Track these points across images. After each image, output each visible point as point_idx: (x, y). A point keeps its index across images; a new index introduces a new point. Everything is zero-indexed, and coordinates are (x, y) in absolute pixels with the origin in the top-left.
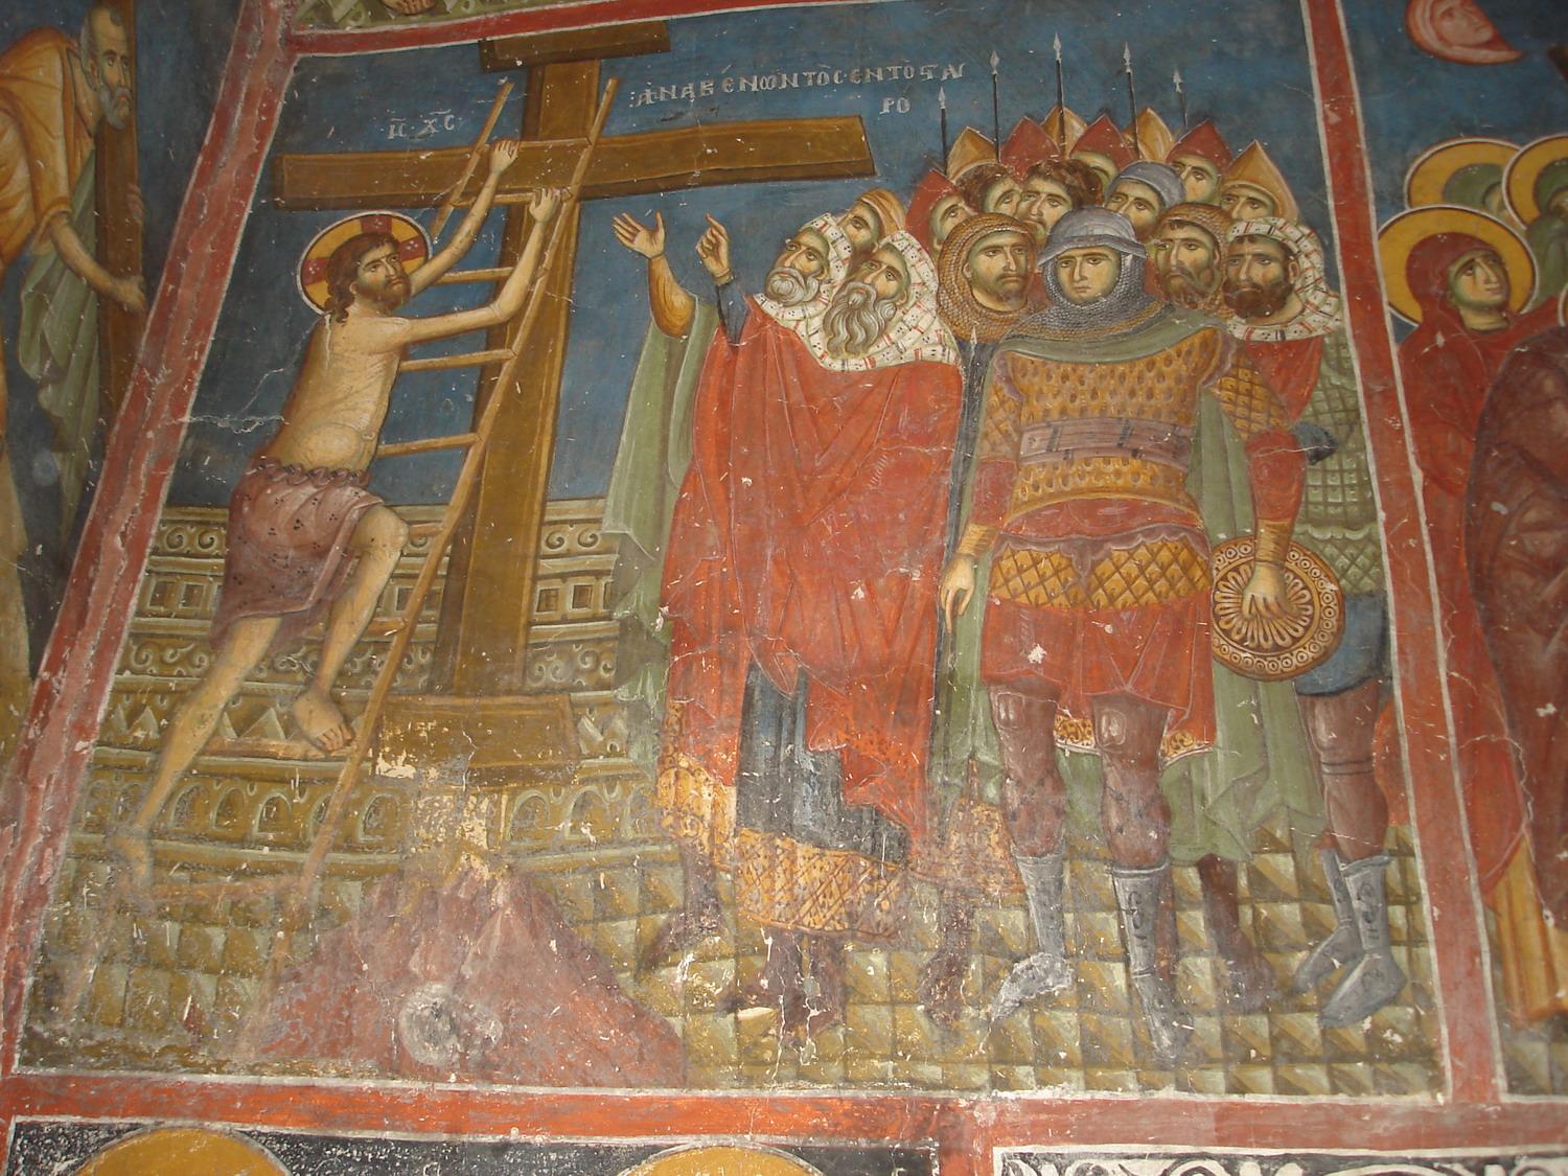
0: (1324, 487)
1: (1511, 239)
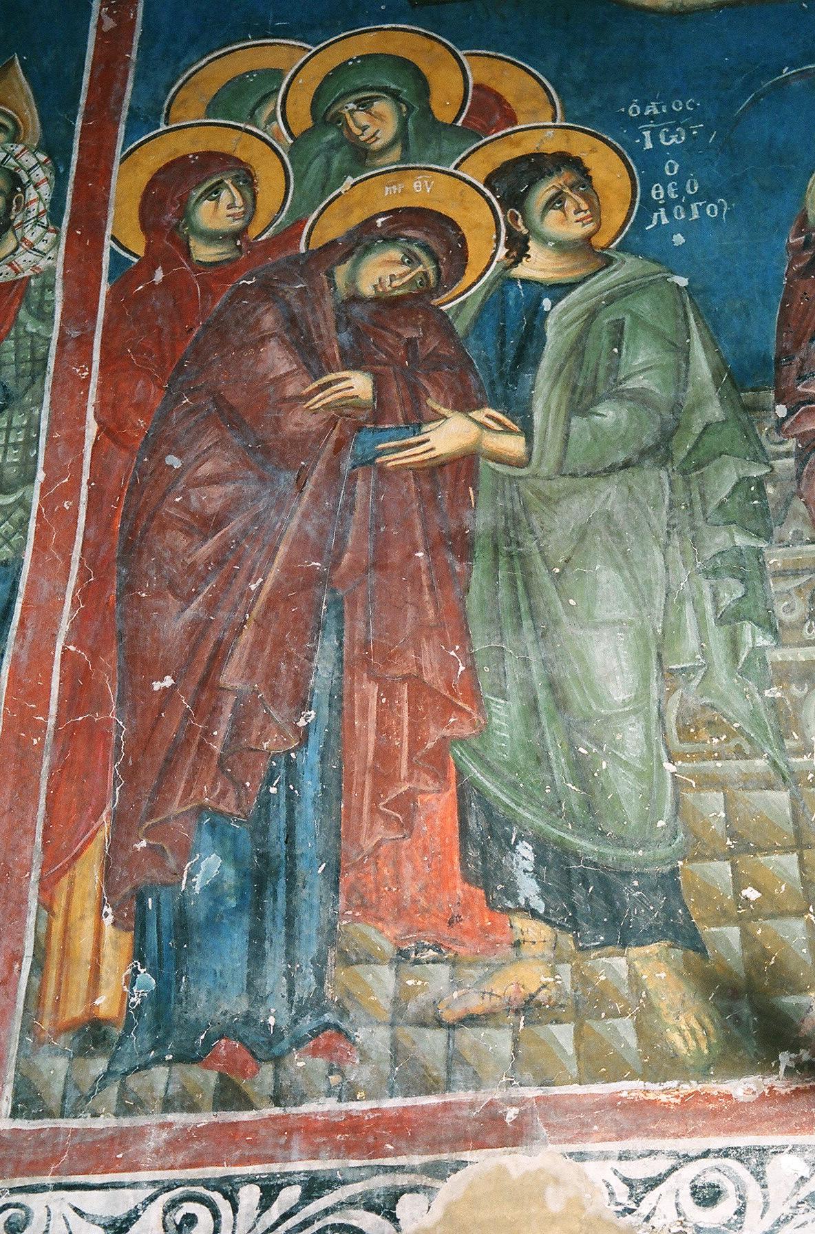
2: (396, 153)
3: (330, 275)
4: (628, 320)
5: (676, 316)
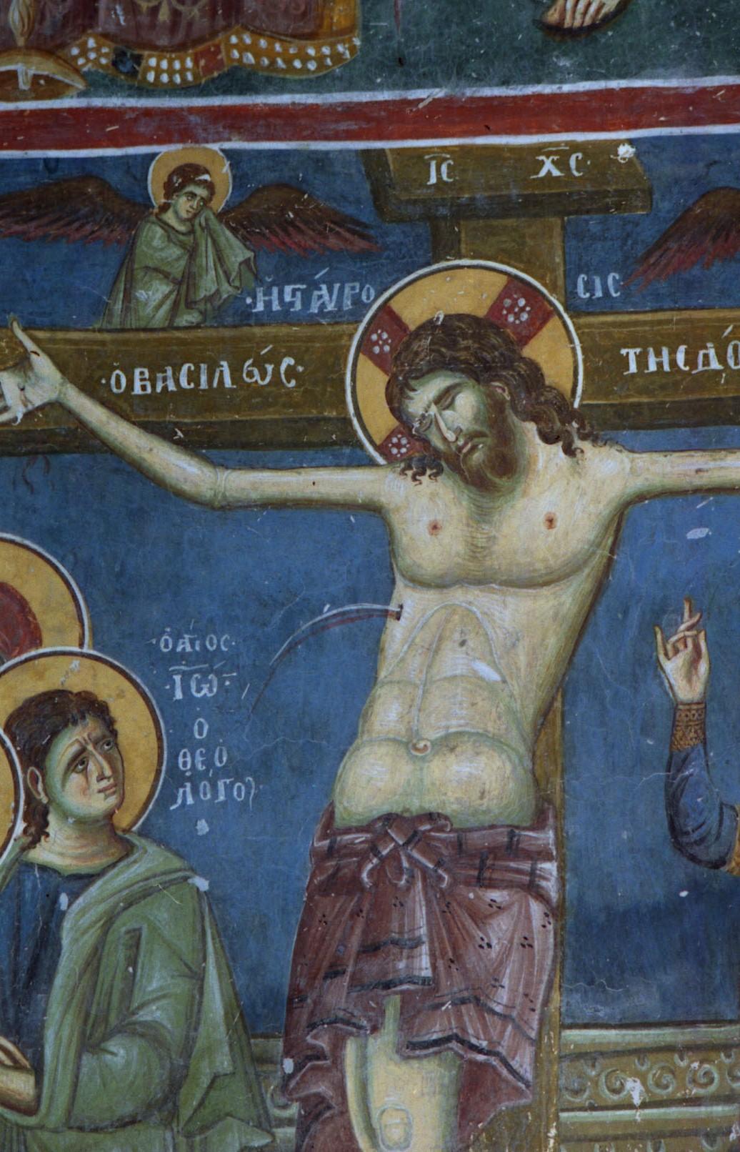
4: (145, 926)
5: (194, 931)
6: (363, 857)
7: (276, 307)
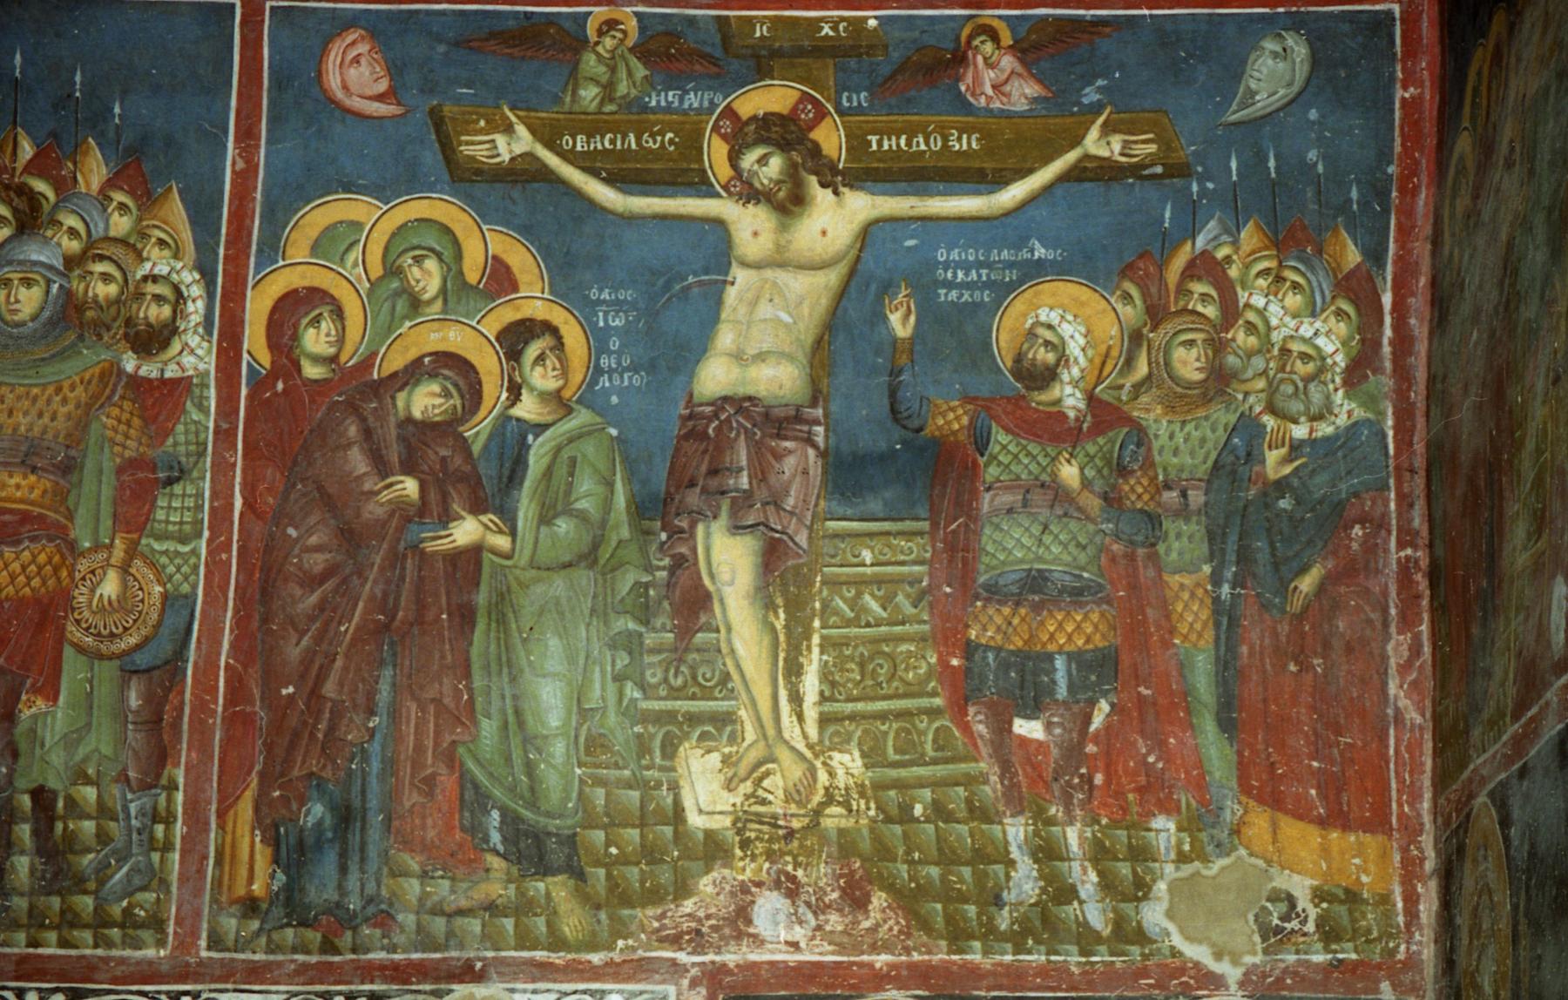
0: (170, 509)
1: (355, 295)
2: (438, 305)
3: (393, 398)
6: (710, 420)
7: (663, 104)
